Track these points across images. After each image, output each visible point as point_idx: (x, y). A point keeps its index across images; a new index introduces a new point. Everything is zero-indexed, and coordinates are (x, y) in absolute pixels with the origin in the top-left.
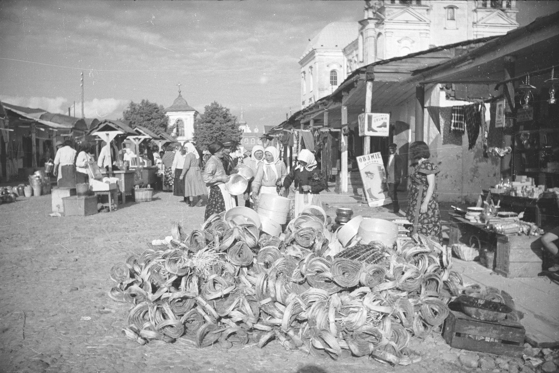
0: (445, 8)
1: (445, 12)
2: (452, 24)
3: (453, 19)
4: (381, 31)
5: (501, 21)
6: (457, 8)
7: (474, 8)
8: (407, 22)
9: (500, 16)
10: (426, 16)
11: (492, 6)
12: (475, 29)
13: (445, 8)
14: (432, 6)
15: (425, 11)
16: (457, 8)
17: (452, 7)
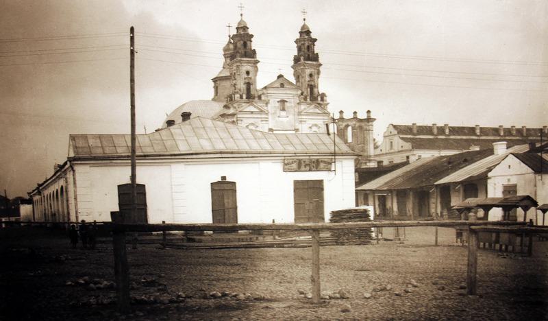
0: (278, 102)
1: (278, 104)
2: (283, 113)
3: (283, 109)
4: (235, 119)
5: (317, 111)
6: (287, 102)
7: (298, 101)
8: (252, 112)
9: (316, 107)
10: (265, 108)
11: (311, 100)
12: (300, 117)
13: (278, 102)
14: (269, 101)
15: (265, 105)
16: (287, 102)
17: (283, 102)
